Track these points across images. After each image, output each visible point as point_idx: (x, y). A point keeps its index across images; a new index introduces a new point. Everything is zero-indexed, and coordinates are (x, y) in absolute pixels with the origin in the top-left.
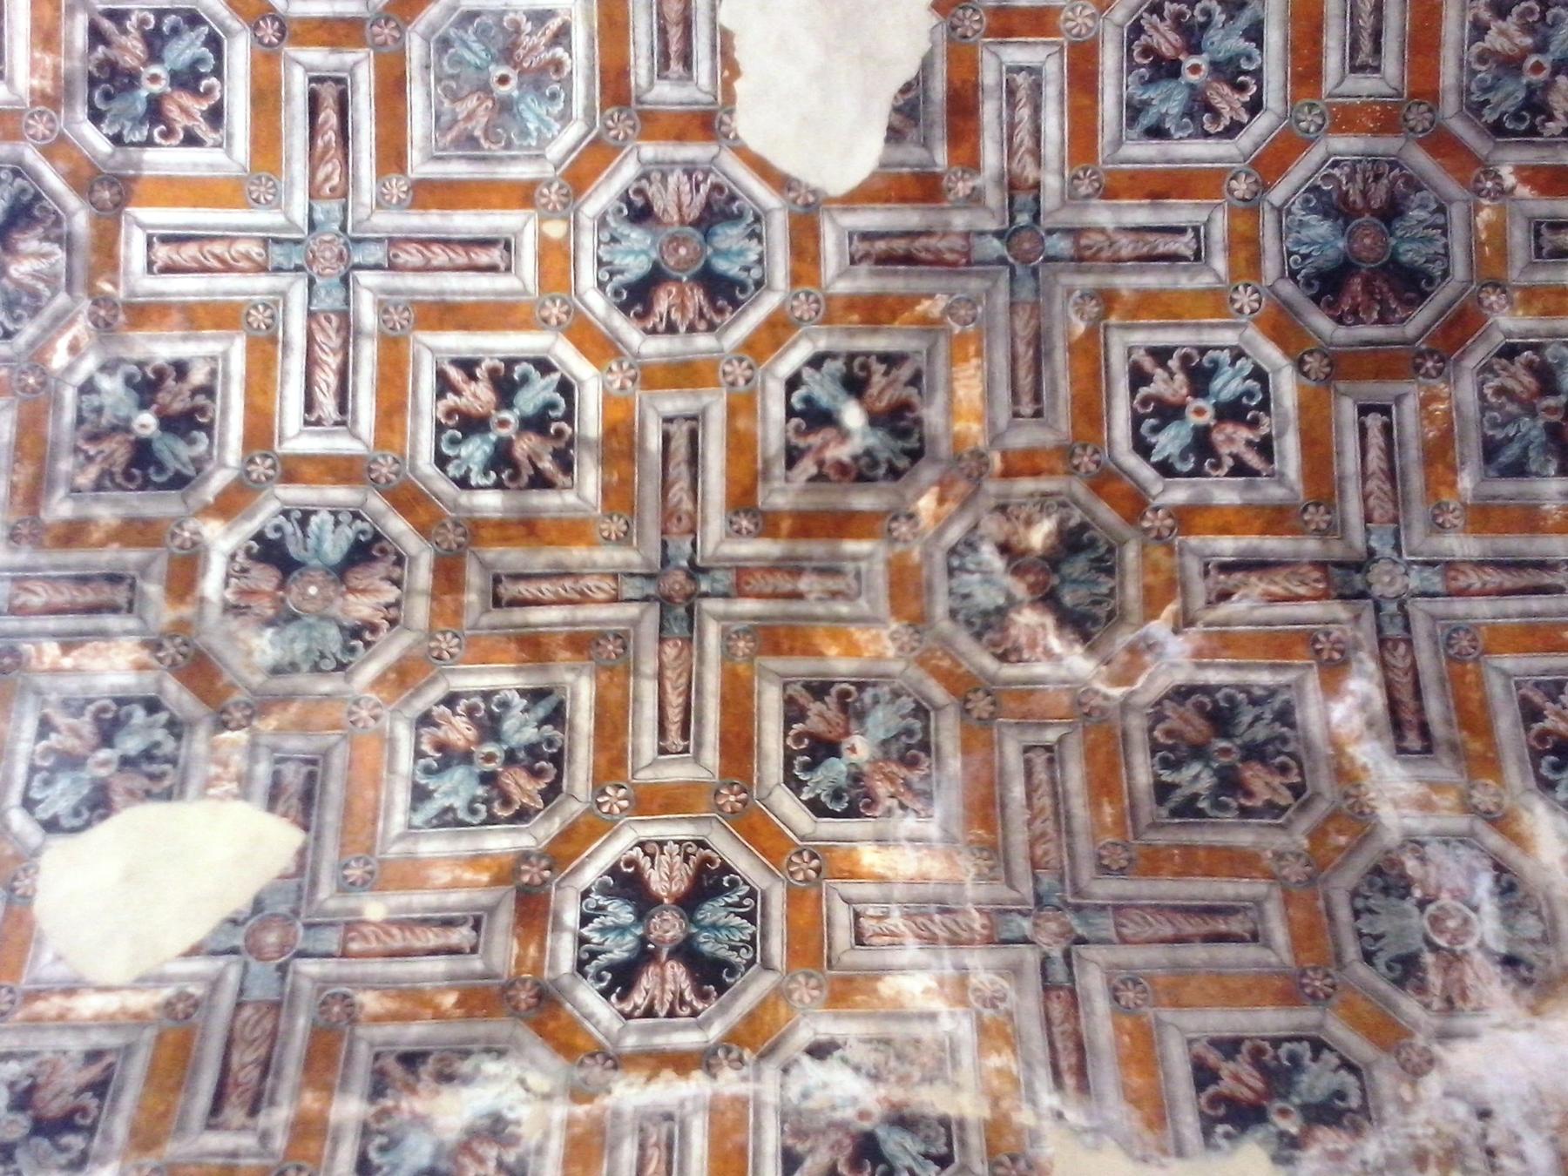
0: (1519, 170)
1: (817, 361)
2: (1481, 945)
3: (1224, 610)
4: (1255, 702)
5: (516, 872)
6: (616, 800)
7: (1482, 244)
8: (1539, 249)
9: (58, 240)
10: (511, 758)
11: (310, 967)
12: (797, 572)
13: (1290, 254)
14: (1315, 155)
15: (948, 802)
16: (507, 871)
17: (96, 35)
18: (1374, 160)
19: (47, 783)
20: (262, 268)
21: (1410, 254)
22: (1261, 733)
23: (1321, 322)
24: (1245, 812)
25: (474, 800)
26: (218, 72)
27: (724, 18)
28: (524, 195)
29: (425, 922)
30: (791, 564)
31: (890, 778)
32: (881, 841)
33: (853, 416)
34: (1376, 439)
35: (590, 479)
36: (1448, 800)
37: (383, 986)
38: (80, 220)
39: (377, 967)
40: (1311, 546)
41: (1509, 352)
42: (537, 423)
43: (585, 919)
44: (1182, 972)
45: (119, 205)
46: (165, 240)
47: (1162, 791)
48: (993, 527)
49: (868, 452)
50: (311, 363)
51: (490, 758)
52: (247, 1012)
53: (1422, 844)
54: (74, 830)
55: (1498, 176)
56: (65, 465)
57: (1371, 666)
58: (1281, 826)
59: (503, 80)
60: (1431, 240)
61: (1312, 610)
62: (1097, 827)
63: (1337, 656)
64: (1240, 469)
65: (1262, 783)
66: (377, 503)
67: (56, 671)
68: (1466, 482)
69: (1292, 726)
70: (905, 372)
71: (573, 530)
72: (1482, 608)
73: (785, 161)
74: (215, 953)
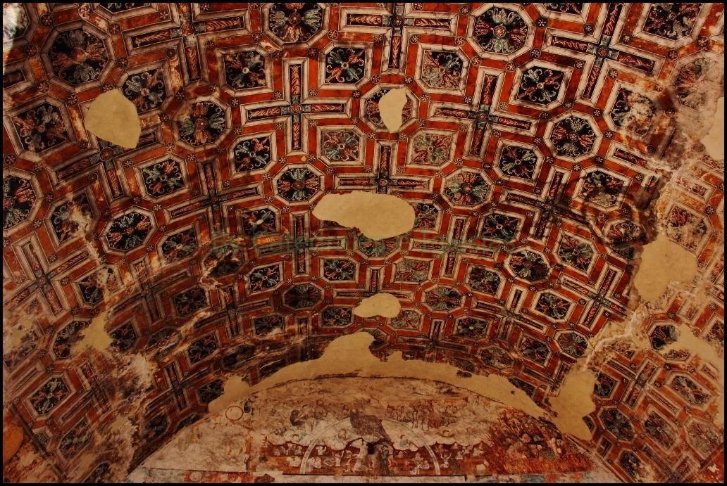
1: (273, 213)
3: (222, 291)
4: (203, 302)
5: (135, 197)
6: (158, 208)
9: (299, 40)
10: (163, 183)
11: (102, 166)
12: (220, 222)
15: (169, 265)
16: (136, 194)
17: (358, 50)
19: (137, 80)
20: (292, 94)
21: (300, 303)
22: (196, 304)
24: (179, 309)
25: (152, 179)
26: (346, 82)
27: (354, 191)
28: (312, 151)
29: (119, 184)
30: (222, 219)
31: (174, 254)
32: (159, 259)
33: (259, 222)
35: (240, 175)
36: (188, 333)
37: (102, 185)
38: (305, 46)
39: (105, 180)
41: (281, 318)
42: (253, 161)
43: (128, 215)
44: (144, 313)
45: (310, 57)
46: (300, 69)
47: (181, 296)
48: (236, 251)
49: (251, 226)
50: (266, 109)
51: (163, 178)
52: (87, 160)
54: (125, 94)
56: (232, 52)
59: (342, 146)
61: (223, 303)
62: (170, 289)
64: (253, 287)
65: (186, 307)
66: (228, 131)
67: (170, 67)
70: (271, 229)
71: (226, 174)
72: (228, 325)
73: (320, 203)
74: (99, 145)
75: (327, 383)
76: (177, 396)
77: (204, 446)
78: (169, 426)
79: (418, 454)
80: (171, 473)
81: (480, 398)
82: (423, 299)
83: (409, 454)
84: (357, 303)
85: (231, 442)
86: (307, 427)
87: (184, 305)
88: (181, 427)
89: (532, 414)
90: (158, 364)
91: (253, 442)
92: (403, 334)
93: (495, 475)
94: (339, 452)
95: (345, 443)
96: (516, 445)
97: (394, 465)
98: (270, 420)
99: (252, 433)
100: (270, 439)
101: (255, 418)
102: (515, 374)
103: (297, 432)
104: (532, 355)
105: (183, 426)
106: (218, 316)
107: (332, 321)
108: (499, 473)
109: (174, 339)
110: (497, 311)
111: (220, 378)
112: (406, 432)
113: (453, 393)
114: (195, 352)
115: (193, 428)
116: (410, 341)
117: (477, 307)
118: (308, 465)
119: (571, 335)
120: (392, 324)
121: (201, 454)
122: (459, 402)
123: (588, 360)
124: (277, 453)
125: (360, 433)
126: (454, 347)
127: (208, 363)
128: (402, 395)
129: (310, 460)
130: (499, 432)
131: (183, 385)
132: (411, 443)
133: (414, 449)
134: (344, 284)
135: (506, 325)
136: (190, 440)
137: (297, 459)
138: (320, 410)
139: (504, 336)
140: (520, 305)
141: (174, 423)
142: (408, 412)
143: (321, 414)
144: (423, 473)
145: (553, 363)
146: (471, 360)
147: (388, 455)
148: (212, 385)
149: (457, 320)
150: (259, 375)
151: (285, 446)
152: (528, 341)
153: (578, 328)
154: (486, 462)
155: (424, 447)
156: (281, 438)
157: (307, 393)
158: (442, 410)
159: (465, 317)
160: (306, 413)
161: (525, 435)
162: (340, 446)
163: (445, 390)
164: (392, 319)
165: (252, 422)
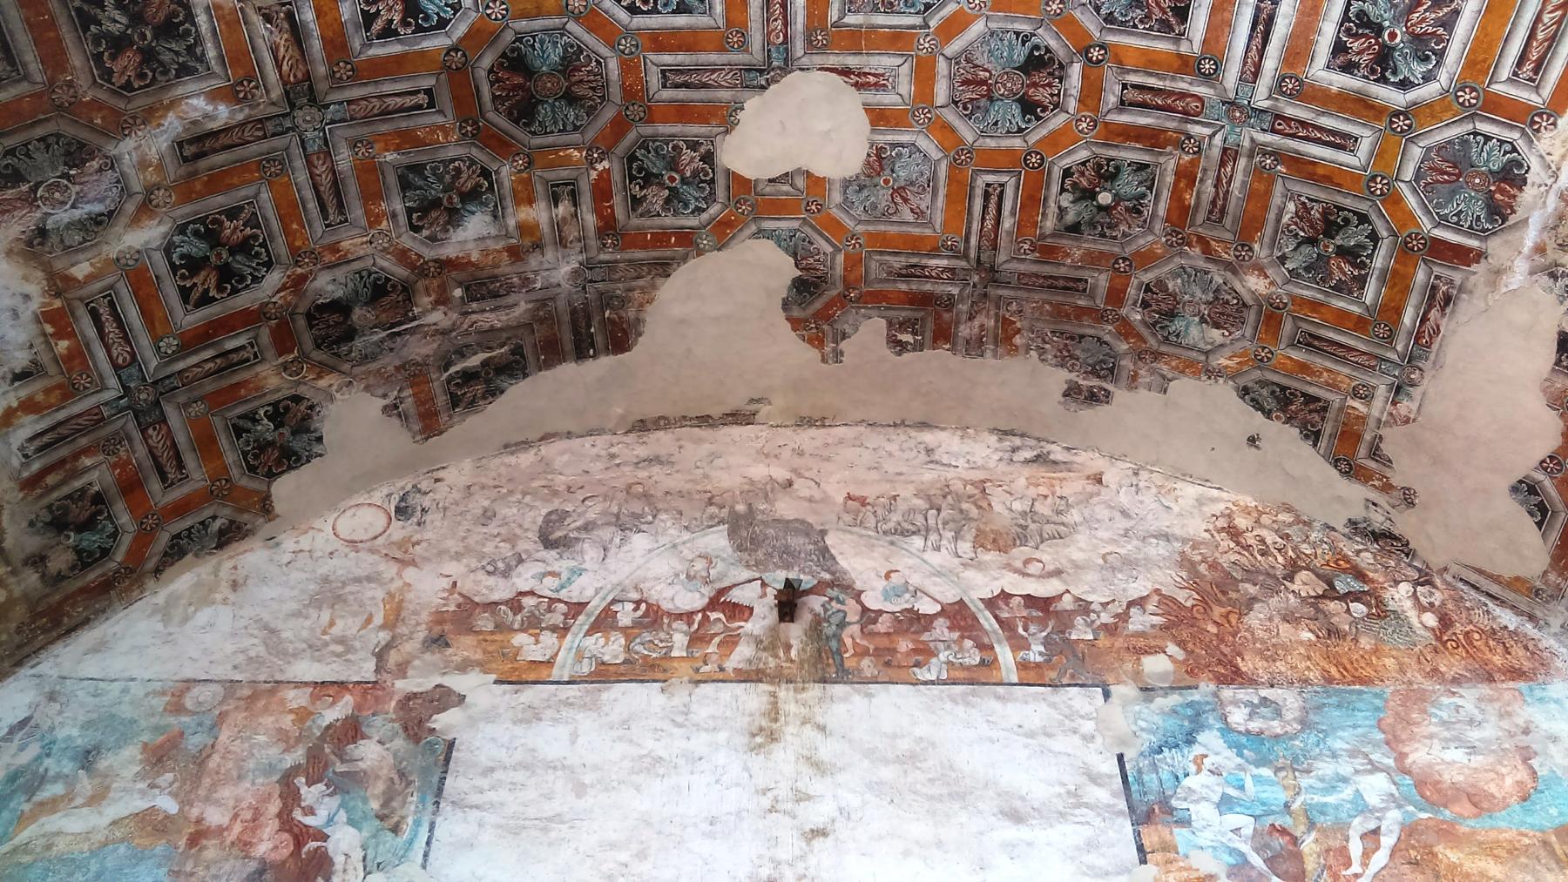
0: (607, 171)
2: (48, 215)
3: (257, 20)
4: (190, 49)
7: (556, 154)
8: (558, 185)
13: (533, 37)
14: (604, 51)
18: (606, 85)
21: (544, 111)
22: (166, 57)
23: (487, 61)
24: (98, 58)
34: (409, 101)
36: (151, 176)
40: (321, 70)
41: (486, 173)
53: (112, 167)
55: (602, 160)
57: (240, 117)
58: (95, 81)
60: (555, 123)
61: (272, 75)
63: (241, 95)
64: (369, 19)
65: (126, 65)
68: (390, 157)
69: (178, 76)
72: (302, 176)
75: (661, 441)
76: (143, 431)
77: (248, 612)
78: (126, 541)
80: (125, 691)
81: (1144, 475)
82: (941, 92)
83: (914, 621)
84: (729, 126)
85: (339, 599)
86: (590, 553)
87: (119, 44)
88: (176, 552)
89: (1320, 518)
90: (51, 276)
91: (410, 596)
92: (882, 243)
93: (1206, 687)
94: (688, 616)
95: (708, 592)
96: (1274, 601)
97: (862, 653)
98: (471, 541)
99: (410, 574)
100: (466, 586)
101: (428, 535)
102: (1260, 362)
103: (556, 567)
104: (1317, 269)
105: (182, 553)
106: (260, 126)
107: (655, 197)
108: (1222, 680)
109: (96, 191)
110: (1191, 110)
111: (303, 390)
112: (903, 562)
113: (1055, 463)
114: (194, 265)
115: (219, 564)
116: (908, 274)
117: (1123, 105)
118: (580, 656)
119: (1464, 142)
120: (847, 205)
121: (234, 635)
122: (1073, 486)
123: (1531, 236)
124: (485, 622)
126: (1051, 284)
127: (249, 318)
128: (890, 467)
129: (590, 641)
130: (1214, 566)
131: (163, 387)
133: (927, 607)
134: (677, 31)
135: (1223, 164)
136: (203, 596)
137: (548, 639)
138: (636, 506)
139: (1218, 211)
140: (1270, 64)
141: (144, 537)
143: (637, 516)
145: (1397, 281)
146: (1107, 331)
147: (842, 625)
148: (278, 414)
149: (1057, 173)
150: (442, 400)
151: (515, 604)
152: (1303, 213)
153: (1495, 106)
154: (1172, 649)
156: (501, 582)
158: (1017, 506)
159: (1083, 154)
160: (591, 515)
161: (1303, 575)
162: (692, 600)
163: (1028, 454)
164: (846, 184)
165: (418, 543)
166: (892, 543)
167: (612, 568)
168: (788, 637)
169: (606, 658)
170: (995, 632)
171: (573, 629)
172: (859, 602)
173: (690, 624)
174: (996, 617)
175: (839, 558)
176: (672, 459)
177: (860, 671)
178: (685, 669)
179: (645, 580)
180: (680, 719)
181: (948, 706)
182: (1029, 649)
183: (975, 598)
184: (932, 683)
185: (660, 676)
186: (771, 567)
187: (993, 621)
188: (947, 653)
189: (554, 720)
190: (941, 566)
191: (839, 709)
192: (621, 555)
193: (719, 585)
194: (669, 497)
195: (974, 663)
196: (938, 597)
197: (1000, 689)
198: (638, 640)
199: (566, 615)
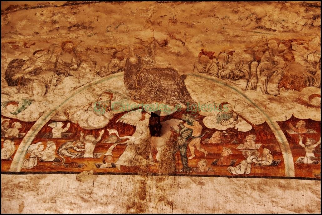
79: (251, 139)
86: (37, 89)
94: (95, 132)
95: (109, 116)
97: (199, 157)
103: (15, 98)
112: (230, 98)
118: (28, 156)
125: (141, 98)
129: (35, 146)
132: (239, 117)
133: (243, 127)
138: (68, 58)
142: (242, 62)
143: (67, 65)
144: (258, 171)
147: (189, 138)
155: (265, 124)
157: (46, 29)
160: (39, 64)
166: (226, 85)
167: (51, 99)
168: (155, 146)
169: (44, 158)
170: (284, 144)
171: (25, 138)
172: (202, 124)
173: (96, 137)
174: (286, 134)
175: (192, 95)
176: (93, 25)
177: (197, 168)
178: (91, 165)
179: (71, 107)
180: (86, 197)
181: (249, 191)
182: (304, 155)
183: (274, 121)
184: (241, 176)
185: (76, 169)
186: (149, 100)
187: (284, 137)
188: (252, 157)
189: (9, 196)
190: (256, 100)
191: (183, 192)
192: (56, 91)
193: (115, 112)
194: (89, 52)
195: (268, 164)
196: (251, 121)
197: (282, 181)
198: (64, 147)
199: (20, 130)
